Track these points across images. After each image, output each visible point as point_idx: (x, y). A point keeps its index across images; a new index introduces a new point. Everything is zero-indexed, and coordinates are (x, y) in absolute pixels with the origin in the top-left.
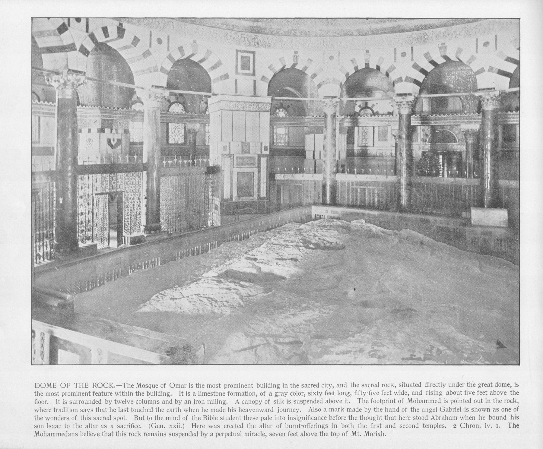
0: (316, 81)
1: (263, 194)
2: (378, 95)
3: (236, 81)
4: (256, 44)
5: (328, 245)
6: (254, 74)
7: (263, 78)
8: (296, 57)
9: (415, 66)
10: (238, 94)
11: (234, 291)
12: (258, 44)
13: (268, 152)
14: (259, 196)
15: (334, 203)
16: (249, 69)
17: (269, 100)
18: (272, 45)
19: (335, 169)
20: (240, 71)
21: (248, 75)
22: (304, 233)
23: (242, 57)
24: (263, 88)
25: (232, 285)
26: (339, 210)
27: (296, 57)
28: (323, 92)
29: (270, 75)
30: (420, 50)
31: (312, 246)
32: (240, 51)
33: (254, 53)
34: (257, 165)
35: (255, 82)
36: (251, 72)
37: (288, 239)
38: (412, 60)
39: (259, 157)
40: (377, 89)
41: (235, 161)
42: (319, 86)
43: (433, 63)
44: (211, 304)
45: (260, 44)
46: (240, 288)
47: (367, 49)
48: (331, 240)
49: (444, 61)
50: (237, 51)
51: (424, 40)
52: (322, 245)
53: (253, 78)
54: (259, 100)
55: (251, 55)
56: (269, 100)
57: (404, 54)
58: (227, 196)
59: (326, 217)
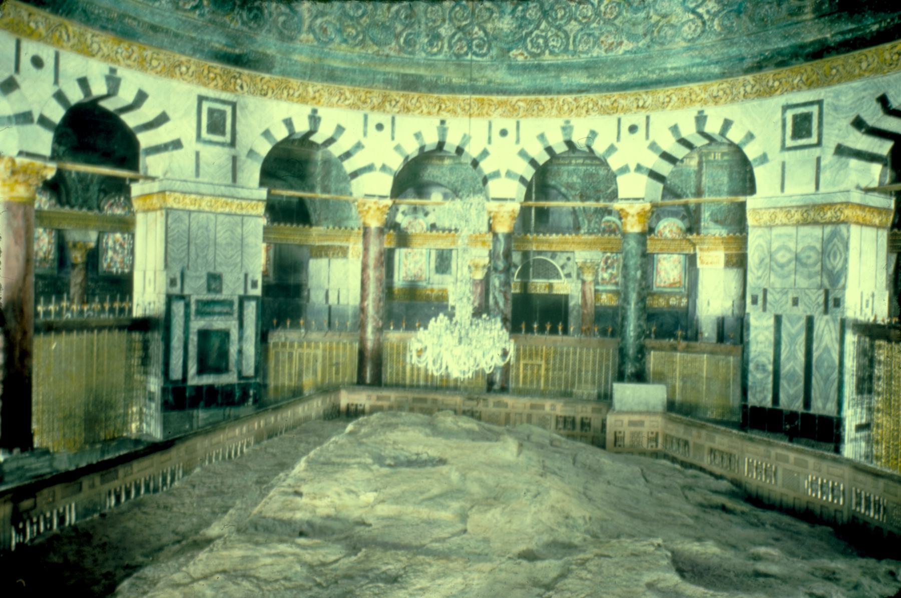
0: (349, 166)
1: (249, 369)
2: (436, 196)
3: (197, 154)
4: (238, 88)
5: (414, 457)
6: (233, 144)
7: (251, 153)
8: (314, 119)
9: (523, 154)
10: (200, 179)
11: (291, 558)
12: (242, 87)
13: (258, 292)
14: (240, 373)
15: (378, 382)
16: (223, 133)
17: (263, 193)
18: (270, 92)
19: (380, 324)
20: (204, 134)
21: (223, 144)
22: (364, 440)
23: (211, 112)
24: (252, 172)
25: (283, 548)
26: (393, 396)
27: (314, 119)
28: (360, 187)
29: (264, 148)
30: (531, 127)
31: (388, 462)
32: (206, 98)
33: (234, 105)
34: (236, 315)
35: (234, 159)
36: (228, 138)
37: (342, 452)
38: (518, 141)
39: (243, 300)
40: (439, 185)
41: (193, 307)
42: (355, 175)
43: (549, 150)
44: (259, 587)
45: (245, 88)
46: (298, 550)
47: (442, 118)
48: (415, 449)
49: (565, 148)
50: (201, 99)
51: (536, 110)
52: (402, 458)
53: (233, 151)
54: (244, 193)
55: (228, 109)
56: (263, 193)
57: (504, 133)
58: (176, 374)
59: (367, 407)
